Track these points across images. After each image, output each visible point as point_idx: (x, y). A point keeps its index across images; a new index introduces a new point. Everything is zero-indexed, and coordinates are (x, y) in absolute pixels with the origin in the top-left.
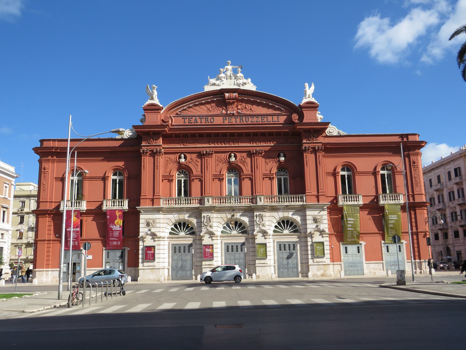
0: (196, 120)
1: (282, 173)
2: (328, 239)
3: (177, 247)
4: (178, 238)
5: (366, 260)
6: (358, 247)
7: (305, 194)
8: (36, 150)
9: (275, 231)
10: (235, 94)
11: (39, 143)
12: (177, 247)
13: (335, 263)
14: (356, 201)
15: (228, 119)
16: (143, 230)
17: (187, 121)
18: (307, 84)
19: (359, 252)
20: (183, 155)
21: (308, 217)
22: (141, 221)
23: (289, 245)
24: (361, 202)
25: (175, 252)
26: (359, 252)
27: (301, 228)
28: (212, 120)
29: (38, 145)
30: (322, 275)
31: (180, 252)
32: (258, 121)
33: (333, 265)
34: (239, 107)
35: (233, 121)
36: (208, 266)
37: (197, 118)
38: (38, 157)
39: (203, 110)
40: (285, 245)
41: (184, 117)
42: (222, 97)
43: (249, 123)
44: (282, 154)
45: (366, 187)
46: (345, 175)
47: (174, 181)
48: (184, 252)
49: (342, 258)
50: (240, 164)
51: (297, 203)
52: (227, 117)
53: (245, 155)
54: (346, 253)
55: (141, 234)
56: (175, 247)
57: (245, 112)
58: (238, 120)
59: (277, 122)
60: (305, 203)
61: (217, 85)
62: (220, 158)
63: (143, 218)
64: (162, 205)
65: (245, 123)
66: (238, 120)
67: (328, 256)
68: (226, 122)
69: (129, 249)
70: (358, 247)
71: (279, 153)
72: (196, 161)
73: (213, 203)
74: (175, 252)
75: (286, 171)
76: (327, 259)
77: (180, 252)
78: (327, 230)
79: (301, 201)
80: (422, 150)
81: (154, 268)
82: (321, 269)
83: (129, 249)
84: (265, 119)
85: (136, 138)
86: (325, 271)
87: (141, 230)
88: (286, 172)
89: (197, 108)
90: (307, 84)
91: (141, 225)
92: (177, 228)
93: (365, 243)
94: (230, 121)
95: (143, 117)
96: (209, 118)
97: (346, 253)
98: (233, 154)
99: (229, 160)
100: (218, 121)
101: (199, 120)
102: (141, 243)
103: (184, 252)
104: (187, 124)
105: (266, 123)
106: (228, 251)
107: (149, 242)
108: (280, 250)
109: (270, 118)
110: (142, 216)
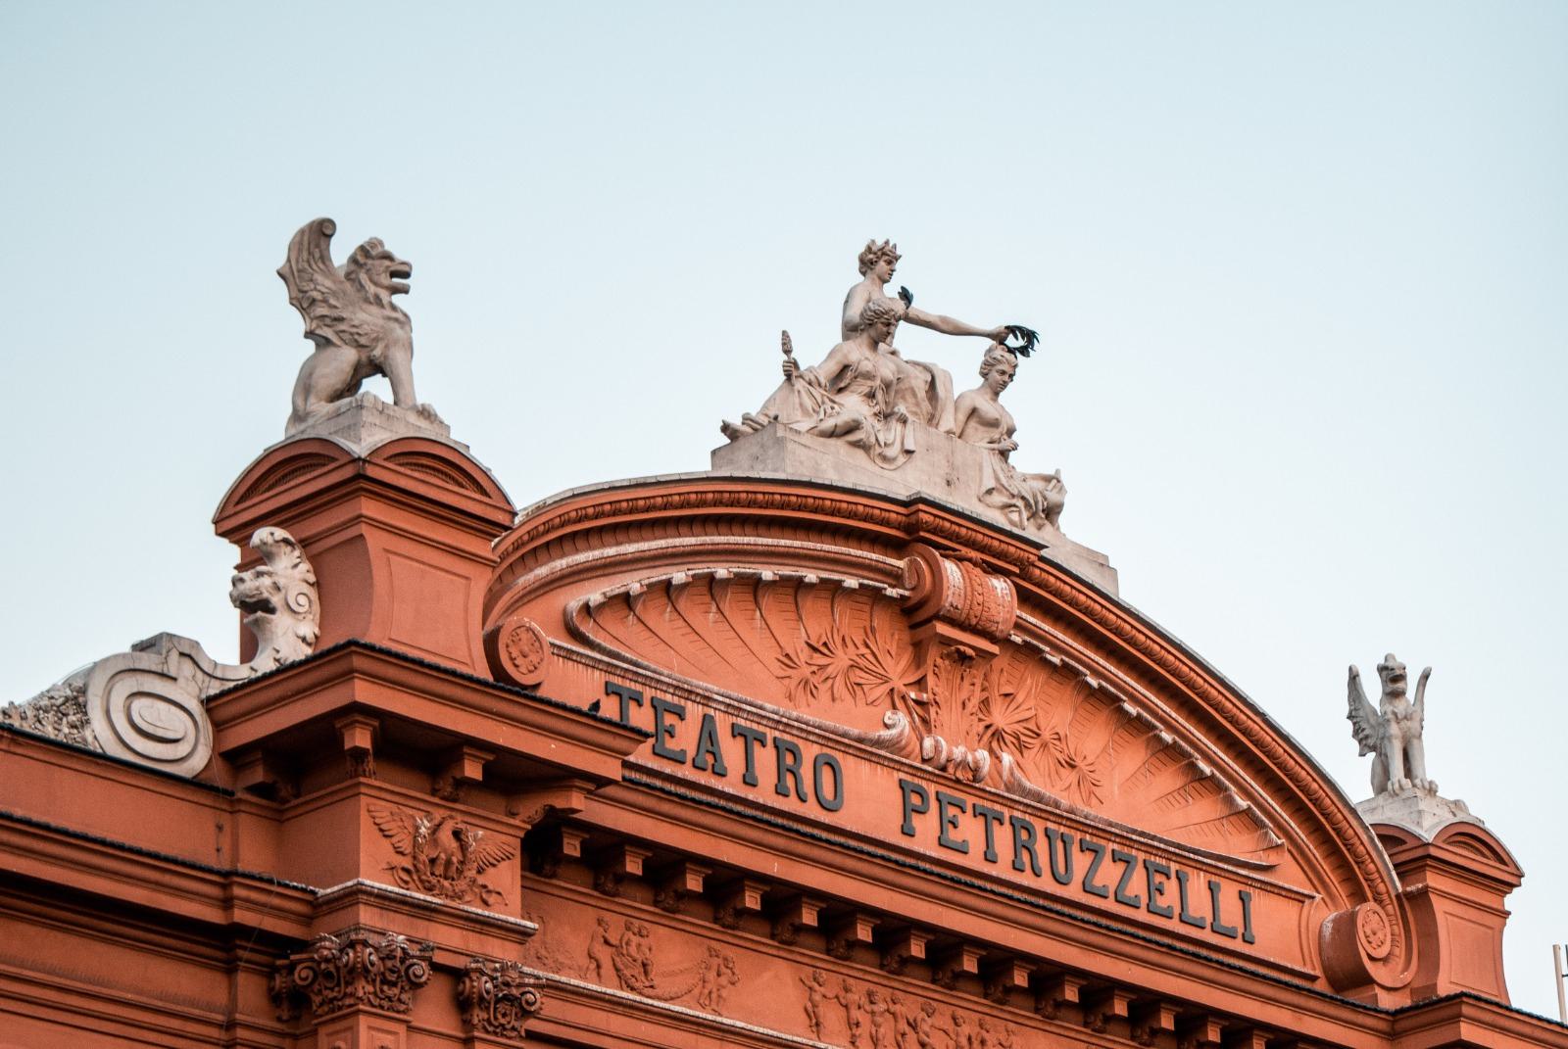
15: (934, 805)
28: (826, 775)
42: (896, 577)
85: (195, 783)
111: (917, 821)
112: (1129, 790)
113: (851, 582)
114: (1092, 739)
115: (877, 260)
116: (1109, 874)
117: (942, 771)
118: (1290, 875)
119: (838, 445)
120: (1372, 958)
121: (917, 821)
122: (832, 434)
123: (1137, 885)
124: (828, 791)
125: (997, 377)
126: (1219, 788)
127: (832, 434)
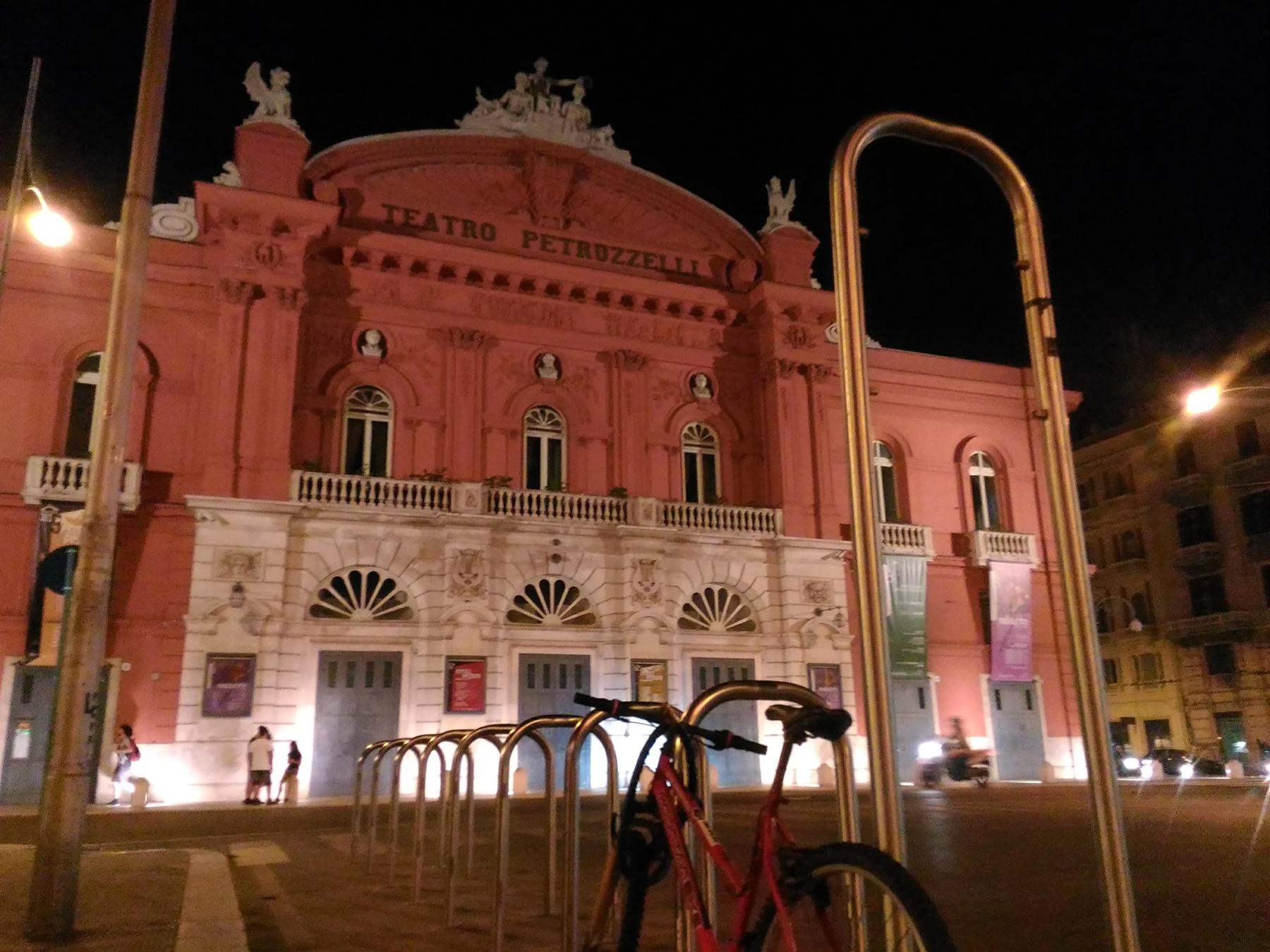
6: (921, 690)
7: (779, 505)
9: (683, 623)
18: (776, 183)
19: (922, 706)
21: (789, 583)
22: (201, 554)
26: (922, 706)
27: (764, 616)
45: (937, 506)
47: (337, 419)
69: (127, 667)
70: (921, 690)
79: (768, 530)
83: (127, 667)
85: (192, 242)
90: (776, 183)
91: (198, 571)
92: (344, 593)
106: (531, 686)
111: (531, 243)
124: (488, 234)
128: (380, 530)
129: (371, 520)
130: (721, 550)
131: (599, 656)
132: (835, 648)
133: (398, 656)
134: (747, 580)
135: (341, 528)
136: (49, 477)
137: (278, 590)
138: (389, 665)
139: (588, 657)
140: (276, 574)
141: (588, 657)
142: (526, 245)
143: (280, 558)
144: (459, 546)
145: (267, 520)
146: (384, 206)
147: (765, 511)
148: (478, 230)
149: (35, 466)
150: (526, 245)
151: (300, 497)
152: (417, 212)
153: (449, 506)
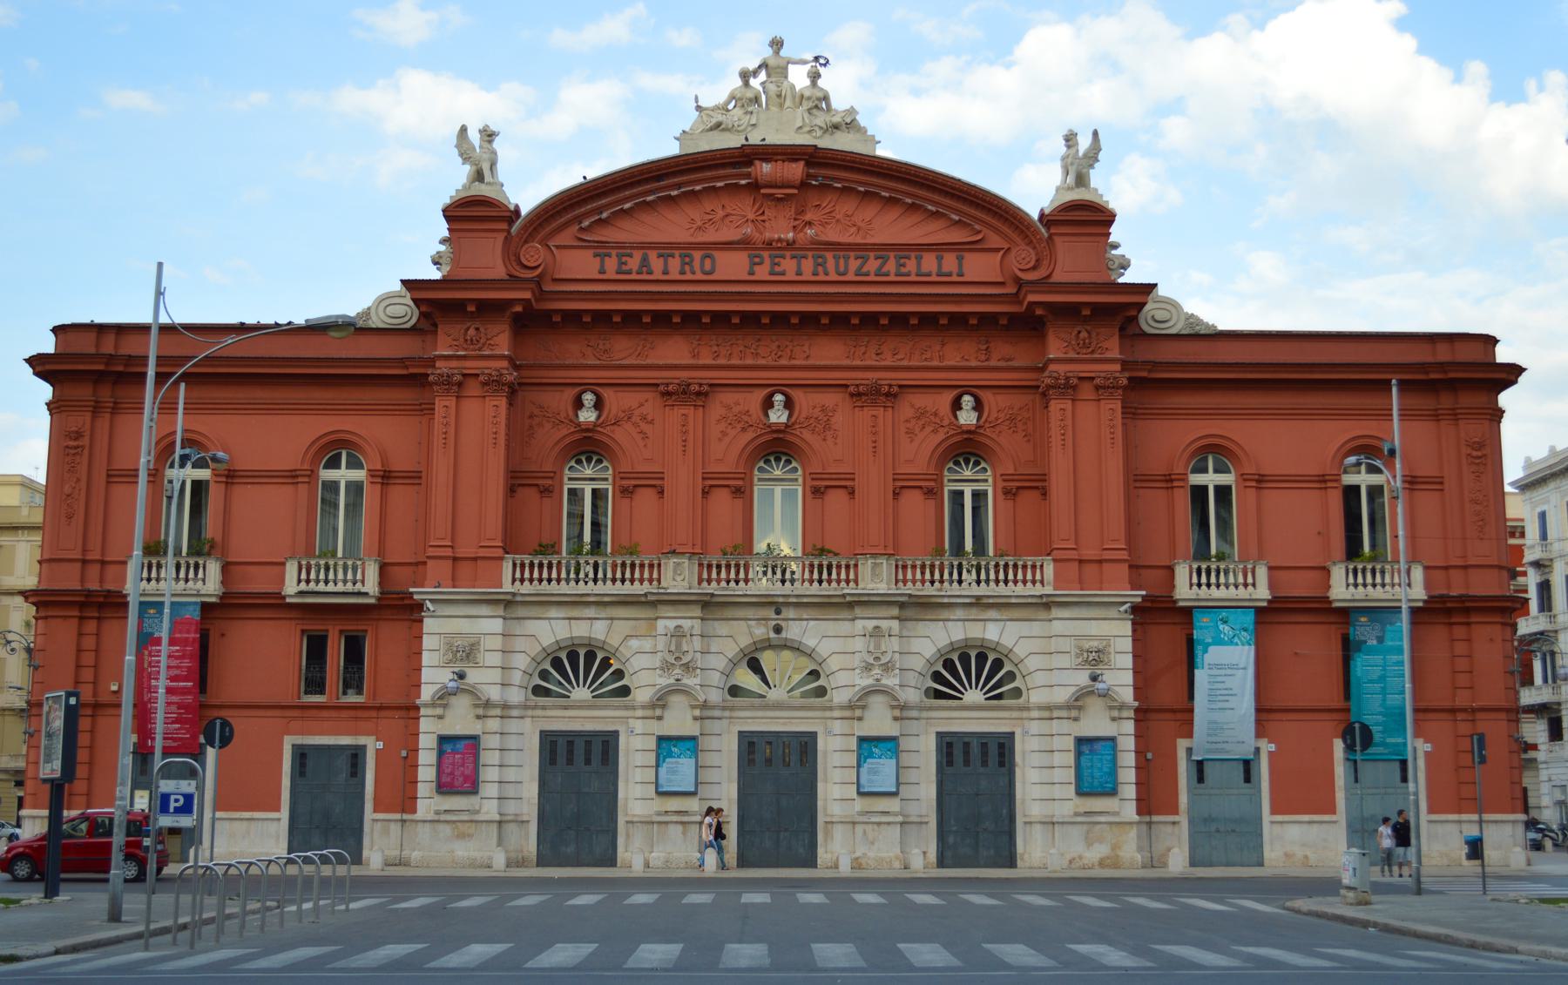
0: (645, 260)
1: (968, 473)
2: (1129, 727)
3: (561, 742)
4: (566, 708)
5: (1274, 811)
8: (40, 365)
10: (796, 170)
11: (52, 338)
12: (561, 742)
13: (1155, 818)
14: (1246, 585)
15: (767, 262)
16: (434, 675)
17: (611, 264)
19: (1247, 779)
20: (588, 398)
22: (428, 642)
23: (984, 745)
24: (1262, 593)
25: (553, 761)
26: (1247, 779)
29: (48, 345)
30: (1102, 864)
31: (570, 761)
32: (885, 269)
33: (1150, 824)
34: (808, 217)
35: (788, 266)
36: (675, 818)
37: (652, 255)
38: (45, 391)
39: (673, 226)
40: (967, 745)
41: (601, 249)
42: (748, 175)
43: (850, 277)
44: (967, 400)
46: (1206, 488)
48: (588, 762)
49: (1183, 799)
50: (807, 435)
51: (1020, 589)
52: (765, 254)
53: (830, 399)
54: (1201, 779)
55: (426, 693)
56: (554, 744)
57: (832, 235)
58: (808, 265)
59: (955, 278)
60: (1049, 590)
61: (726, 130)
62: (736, 409)
63: (437, 630)
64: (507, 587)
65: (833, 277)
66: (808, 265)
67: (1130, 791)
68: (762, 273)
71: (959, 397)
72: (644, 418)
73: (700, 582)
74: (553, 761)
75: (983, 465)
76: (1125, 805)
77: (570, 761)
78: (1127, 695)
80: (1505, 399)
81: (476, 817)
82: (1101, 841)
83: (380, 745)
84: (911, 265)
85: (413, 329)
86: (1115, 847)
87: (426, 675)
88: (985, 470)
89: (648, 218)
91: (426, 658)
93: (1272, 747)
94: (777, 269)
95: (443, 248)
96: (697, 255)
97: (1201, 779)
98: (779, 398)
99: (767, 415)
100: (732, 266)
101: (657, 264)
102: (424, 724)
103: (588, 762)
104: (611, 275)
105: (913, 278)
107: (460, 720)
108: (950, 763)
109: (929, 262)
110: (429, 624)
112: (890, 227)
113: (698, 188)
114: (869, 211)
115: (777, 44)
116: (872, 265)
117: (769, 245)
118: (995, 240)
119: (715, 133)
120: (1034, 268)
121: (756, 268)
122: (711, 129)
123: (891, 266)
125: (815, 76)
126: (943, 215)
127: (711, 129)
128: (590, 612)
129: (579, 602)
130: (974, 613)
131: (829, 733)
132: (1114, 719)
133: (616, 733)
134: (1007, 641)
135: (553, 612)
136: (304, 576)
137: (496, 675)
138: (606, 744)
139: (814, 735)
140: (495, 659)
141: (814, 735)
142: (751, 273)
143: (497, 642)
144: (672, 624)
145: (484, 610)
146: (596, 255)
147: (1030, 561)
148: (697, 264)
149: (291, 570)
150: (751, 273)
151: (514, 580)
152: (630, 256)
153: (659, 581)
